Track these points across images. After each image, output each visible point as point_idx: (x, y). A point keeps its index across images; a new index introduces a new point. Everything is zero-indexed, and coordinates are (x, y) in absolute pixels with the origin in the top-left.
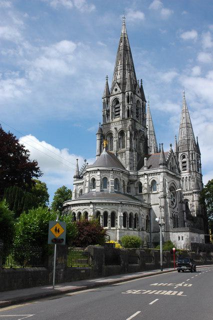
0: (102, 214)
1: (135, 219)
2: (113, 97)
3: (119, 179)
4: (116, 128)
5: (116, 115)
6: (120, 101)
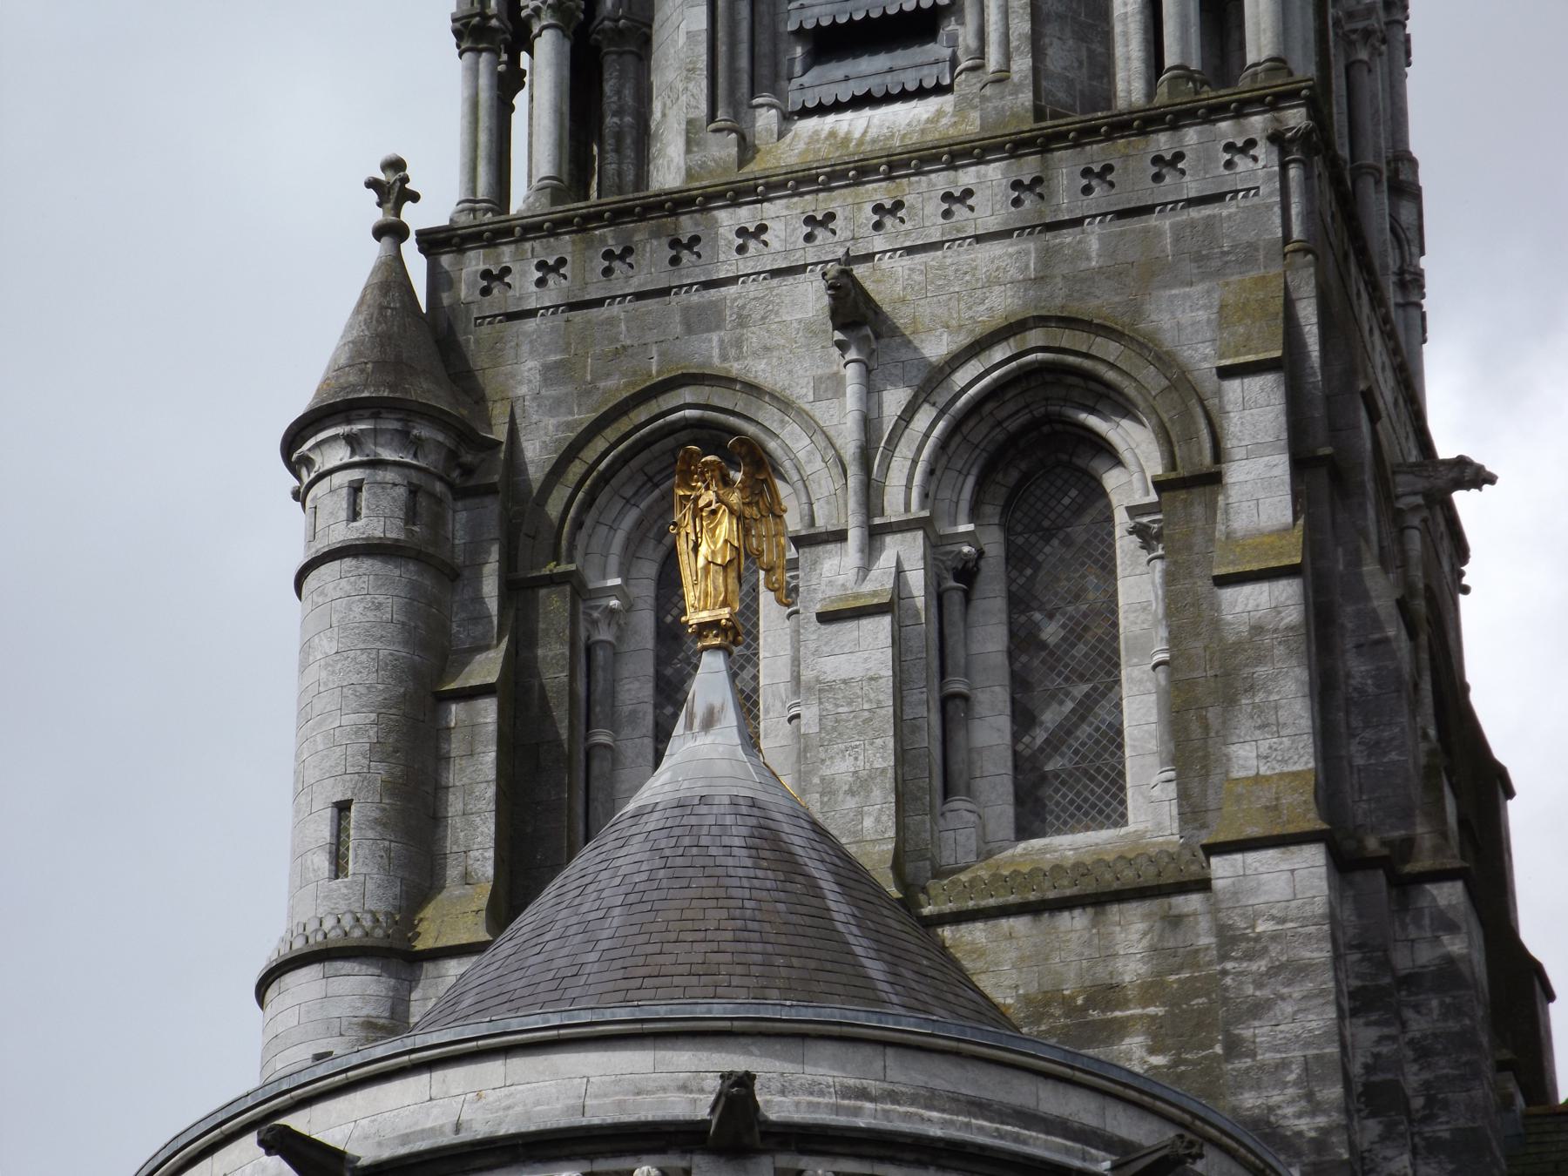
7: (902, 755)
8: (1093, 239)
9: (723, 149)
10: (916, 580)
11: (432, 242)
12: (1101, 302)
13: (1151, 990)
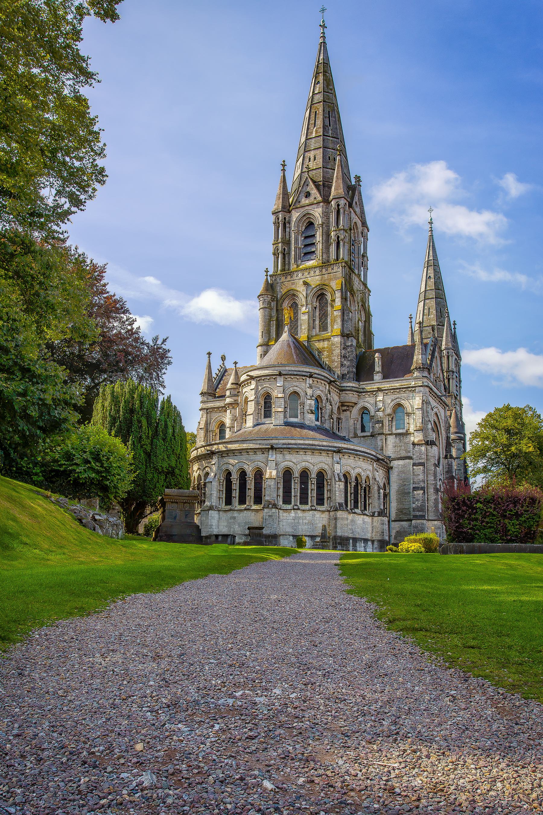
0: (296, 474)
1: (365, 488)
2: (302, 210)
3: (324, 398)
4: (306, 284)
5: (306, 254)
6: (318, 220)
7: (309, 326)
8: (326, 276)
9: (295, 266)
10: (310, 309)
11: (270, 276)
12: (326, 282)
13: (327, 347)
